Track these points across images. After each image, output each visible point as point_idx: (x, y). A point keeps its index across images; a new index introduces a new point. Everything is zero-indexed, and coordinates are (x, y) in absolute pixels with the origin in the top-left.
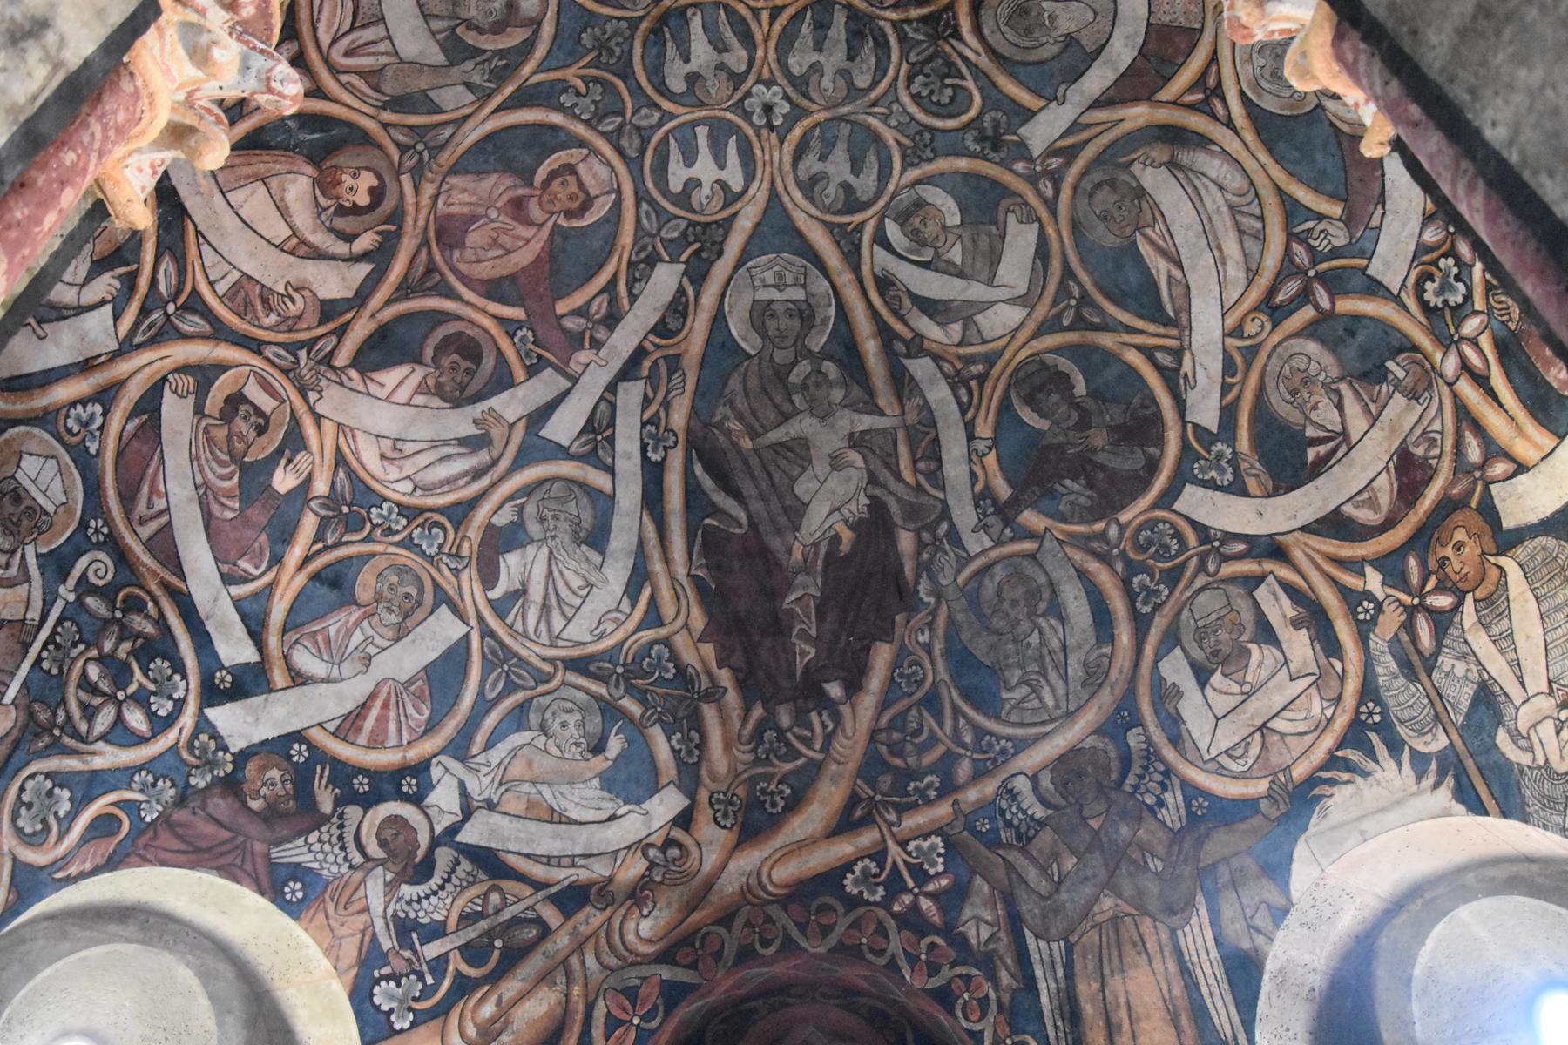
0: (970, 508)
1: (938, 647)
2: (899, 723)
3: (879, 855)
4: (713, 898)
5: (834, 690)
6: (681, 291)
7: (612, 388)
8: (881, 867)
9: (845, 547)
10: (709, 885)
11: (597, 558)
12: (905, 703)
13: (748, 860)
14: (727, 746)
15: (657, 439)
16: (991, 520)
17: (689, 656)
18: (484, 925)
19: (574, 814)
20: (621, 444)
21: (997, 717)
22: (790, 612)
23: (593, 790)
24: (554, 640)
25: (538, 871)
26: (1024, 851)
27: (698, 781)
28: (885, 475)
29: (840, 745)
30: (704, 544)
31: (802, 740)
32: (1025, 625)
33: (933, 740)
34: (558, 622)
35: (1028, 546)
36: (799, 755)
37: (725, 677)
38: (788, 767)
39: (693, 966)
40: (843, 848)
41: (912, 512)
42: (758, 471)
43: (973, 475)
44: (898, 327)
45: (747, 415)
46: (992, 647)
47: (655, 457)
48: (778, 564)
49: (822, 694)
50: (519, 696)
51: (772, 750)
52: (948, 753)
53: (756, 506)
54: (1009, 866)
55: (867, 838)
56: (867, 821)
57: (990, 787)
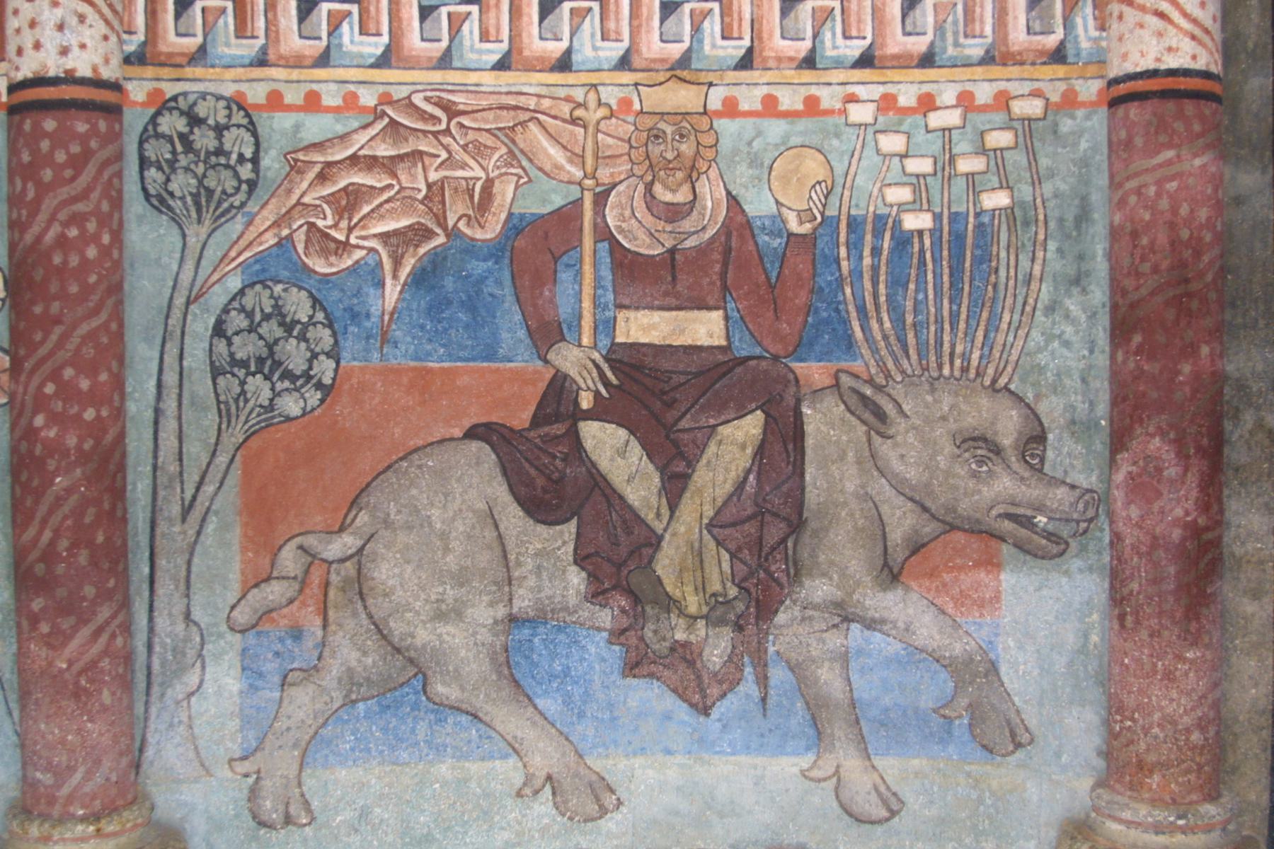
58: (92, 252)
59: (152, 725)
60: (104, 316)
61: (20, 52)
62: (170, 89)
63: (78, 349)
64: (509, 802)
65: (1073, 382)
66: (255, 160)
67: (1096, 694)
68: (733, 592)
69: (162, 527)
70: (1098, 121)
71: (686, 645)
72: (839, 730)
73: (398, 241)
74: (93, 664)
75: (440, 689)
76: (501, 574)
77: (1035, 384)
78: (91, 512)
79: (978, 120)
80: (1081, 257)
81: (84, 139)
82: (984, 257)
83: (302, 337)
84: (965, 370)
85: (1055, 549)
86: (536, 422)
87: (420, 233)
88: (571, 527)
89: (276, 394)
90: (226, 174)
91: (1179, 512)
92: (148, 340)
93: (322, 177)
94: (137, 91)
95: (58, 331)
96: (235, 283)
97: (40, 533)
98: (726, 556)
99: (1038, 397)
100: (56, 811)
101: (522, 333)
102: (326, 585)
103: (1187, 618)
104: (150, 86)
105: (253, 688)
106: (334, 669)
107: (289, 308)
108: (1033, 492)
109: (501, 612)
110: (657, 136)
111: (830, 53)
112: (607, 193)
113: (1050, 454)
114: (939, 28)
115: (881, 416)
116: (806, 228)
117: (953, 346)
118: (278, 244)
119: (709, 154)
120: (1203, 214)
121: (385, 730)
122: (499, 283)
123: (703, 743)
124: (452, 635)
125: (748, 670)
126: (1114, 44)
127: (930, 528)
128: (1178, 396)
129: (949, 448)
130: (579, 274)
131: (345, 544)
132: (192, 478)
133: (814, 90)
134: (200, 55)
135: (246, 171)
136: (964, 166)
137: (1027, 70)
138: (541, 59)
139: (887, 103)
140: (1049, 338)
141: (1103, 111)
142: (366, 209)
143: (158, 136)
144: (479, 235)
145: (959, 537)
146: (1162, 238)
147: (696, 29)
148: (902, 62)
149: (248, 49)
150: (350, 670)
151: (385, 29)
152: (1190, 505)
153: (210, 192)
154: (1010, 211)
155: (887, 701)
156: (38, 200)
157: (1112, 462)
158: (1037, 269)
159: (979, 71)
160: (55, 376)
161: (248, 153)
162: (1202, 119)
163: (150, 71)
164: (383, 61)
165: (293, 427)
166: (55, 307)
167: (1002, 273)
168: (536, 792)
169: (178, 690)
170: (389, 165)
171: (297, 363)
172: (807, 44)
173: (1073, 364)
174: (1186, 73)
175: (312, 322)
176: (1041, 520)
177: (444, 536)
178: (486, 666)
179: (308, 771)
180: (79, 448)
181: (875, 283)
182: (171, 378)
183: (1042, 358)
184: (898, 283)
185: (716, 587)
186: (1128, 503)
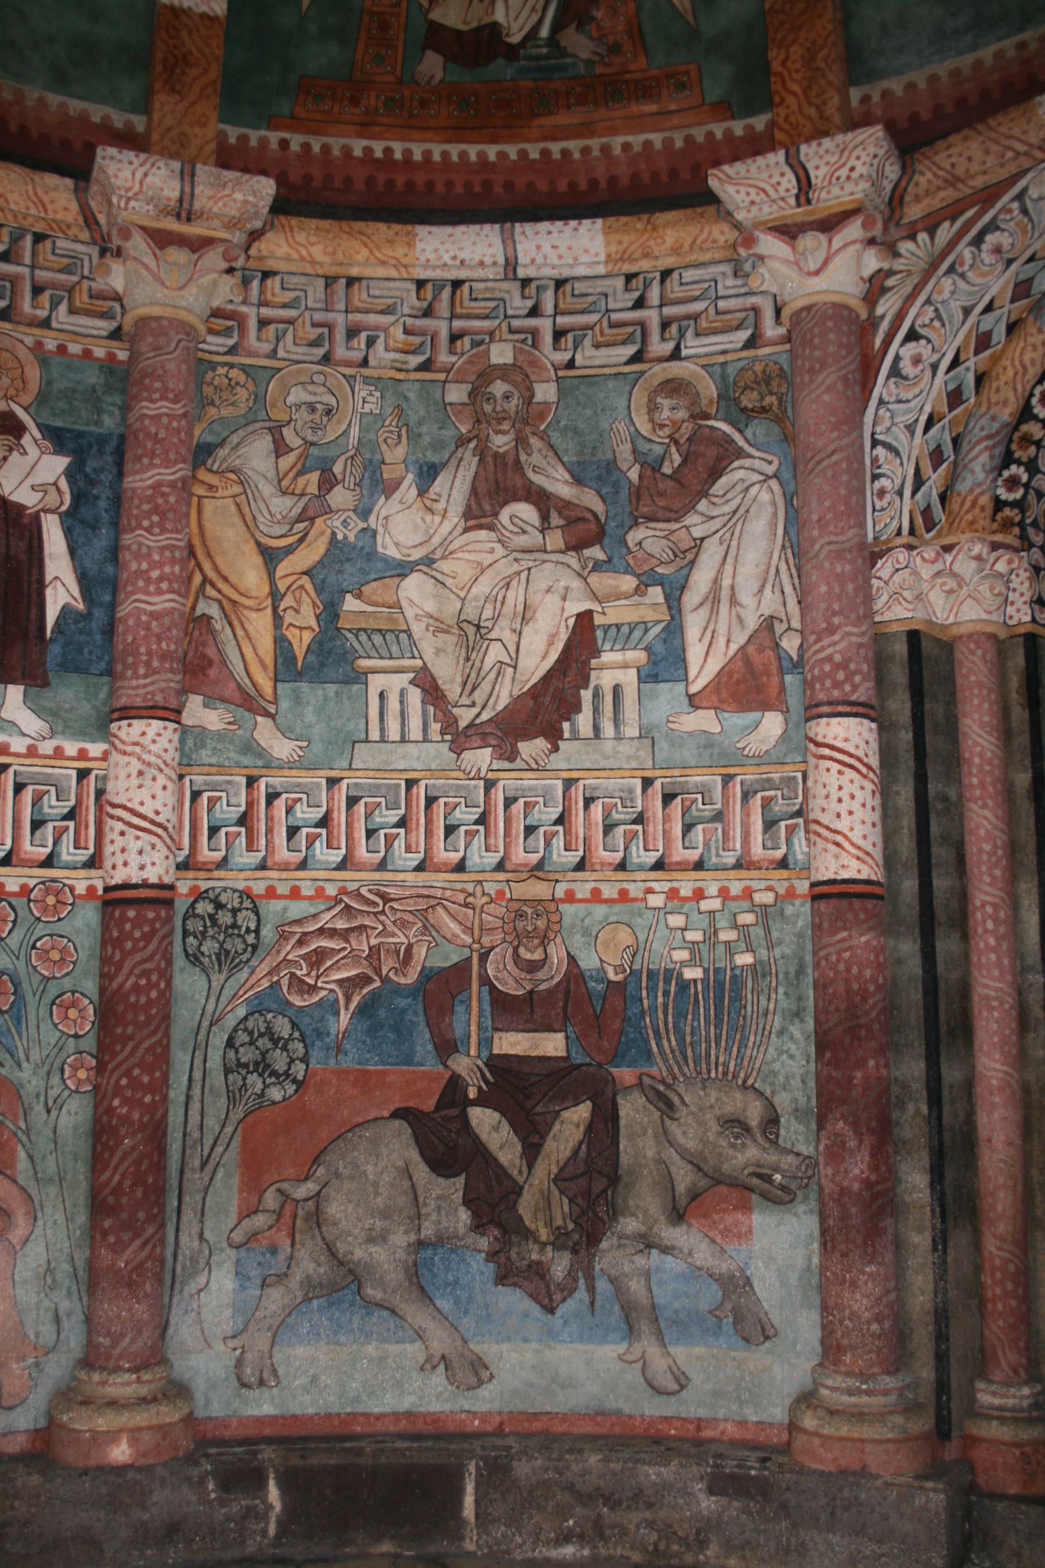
58: (154, 994)
59: (173, 1311)
60: (159, 1035)
61: (114, 867)
62: (204, 885)
63: (143, 1058)
64: (415, 1375)
65: (796, 1083)
66: (257, 931)
68: (571, 1226)
69: (188, 1174)
71: (539, 1263)
72: (644, 1326)
73: (349, 985)
74: (140, 1266)
75: (370, 1291)
76: (413, 1212)
77: (772, 1084)
78: (146, 1162)
79: (733, 906)
80: (800, 998)
81: (152, 923)
82: (737, 998)
83: (285, 1049)
85: (787, 1198)
86: (439, 1107)
87: (363, 980)
88: (461, 1181)
89: (266, 1086)
90: (238, 940)
91: (856, 1171)
92: (184, 1050)
93: (300, 943)
94: (183, 888)
95: (131, 1044)
96: (241, 1012)
97: (112, 1176)
98: (566, 1201)
99: (773, 1093)
100: (111, 1364)
101: (430, 1047)
102: (295, 1216)
104: (190, 883)
105: (243, 1288)
106: (298, 1275)
107: (276, 1029)
108: (773, 1158)
109: (412, 1237)
110: (521, 915)
111: (635, 860)
112: (488, 953)
113: (782, 1132)
114: (707, 844)
115: (670, 1105)
116: (620, 977)
118: (271, 987)
119: (556, 927)
120: (868, 973)
121: (330, 1319)
122: (416, 1013)
123: (550, 1335)
124: (379, 1253)
125: (582, 1282)
127: (704, 1183)
128: (854, 1093)
129: (715, 1127)
130: (469, 1007)
131: (309, 1188)
132: (208, 1142)
133: (625, 885)
134: (223, 863)
135: (251, 939)
136: (723, 936)
137: (763, 873)
138: (445, 864)
139: (673, 894)
140: (780, 1052)
142: (329, 963)
143: (195, 916)
144: (403, 981)
145: (724, 1189)
146: (841, 988)
147: (548, 844)
148: (683, 867)
149: (255, 858)
150: (308, 1277)
151: (343, 844)
152: (864, 1167)
153: (227, 952)
154: (753, 967)
155: (677, 1305)
156: (122, 961)
158: (772, 1006)
159: (732, 874)
160: (128, 1073)
161: (253, 927)
162: (865, 910)
163: (191, 874)
164: (342, 866)
165: (276, 1108)
166: (130, 1029)
168: (434, 1367)
169: (192, 1287)
170: (344, 935)
171: (280, 1066)
172: (621, 854)
173: (796, 1070)
174: (854, 881)
175: (291, 1038)
176: (778, 1177)
177: (375, 1184)
178: (402, 1276)
179: (276, 1348)
180: (140, 1120)
181: (666, 1015)
182: (198, 1075)
183: (777, 1066)
184: (681, 1015)
185: (559, 1222)
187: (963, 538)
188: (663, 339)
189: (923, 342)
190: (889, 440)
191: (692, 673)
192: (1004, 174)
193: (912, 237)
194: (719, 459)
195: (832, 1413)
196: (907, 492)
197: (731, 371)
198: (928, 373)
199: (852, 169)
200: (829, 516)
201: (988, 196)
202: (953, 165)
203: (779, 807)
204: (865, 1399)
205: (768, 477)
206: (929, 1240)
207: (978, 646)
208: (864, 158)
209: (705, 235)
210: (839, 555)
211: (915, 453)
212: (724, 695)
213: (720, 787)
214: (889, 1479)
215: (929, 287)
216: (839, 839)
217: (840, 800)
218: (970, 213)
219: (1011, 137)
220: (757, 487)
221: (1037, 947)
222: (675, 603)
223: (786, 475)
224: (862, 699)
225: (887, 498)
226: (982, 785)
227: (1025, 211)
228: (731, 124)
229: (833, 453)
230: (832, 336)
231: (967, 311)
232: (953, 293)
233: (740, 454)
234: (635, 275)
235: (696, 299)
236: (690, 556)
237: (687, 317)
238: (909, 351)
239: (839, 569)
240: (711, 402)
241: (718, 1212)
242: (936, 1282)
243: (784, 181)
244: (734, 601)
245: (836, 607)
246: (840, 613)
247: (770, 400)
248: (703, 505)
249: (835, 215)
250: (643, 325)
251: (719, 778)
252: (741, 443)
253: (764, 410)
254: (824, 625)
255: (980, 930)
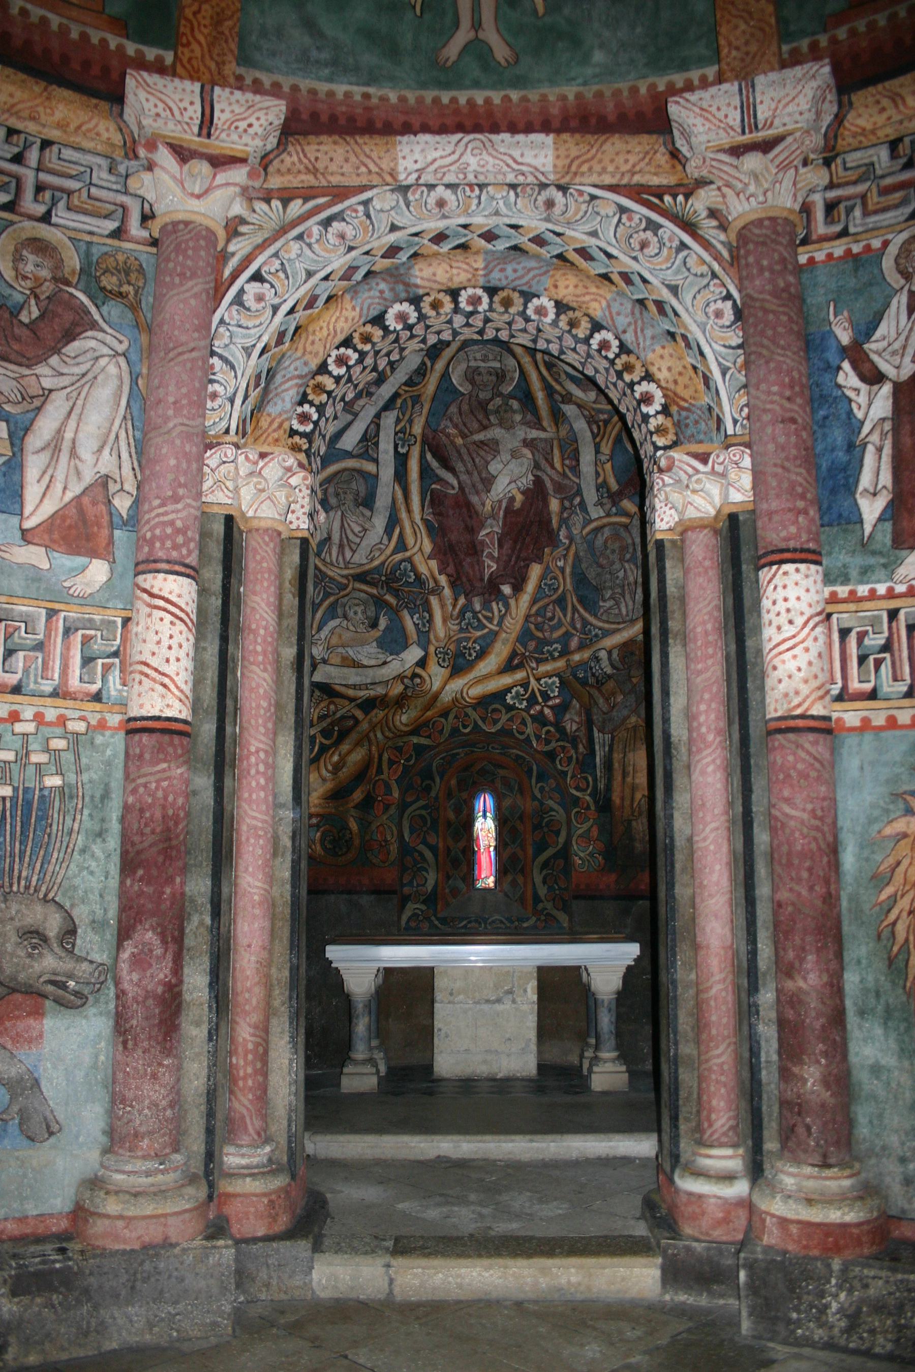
0: (594, 490)
1: (568, 570)
2: (541, 613)
3: (525, 685)
4: (438, 704)
5: (507, 589)
6: (423, 363)
7: (378, 416)
8: (526, 691)
9: (517, 505)
10: (436, 696)
11: (368, 513)
12: (546, 600)
13: (457, 684)
14: (445, 621)
15: (404, 441)
16: (605, 501)
17: (423, 569)
18: (329, 720)
19: (365, 662)
20: (382, 446)
21: (595, 616)
22: (482, 543)
23: (372, 648)
24: (347, 564)
25: (351, 693)
26: (600, 691)
27: (429, 642)
28: (543, 463)
29: (508, 621)
30: (432, 502)
31: (486, 617)
32: (617, 566)
33: (560, 624)
34: (348, 554)
35: (624, 520)
36: (485, 627)
37: (443, 580)
38: (479, 634)
39: (429, 737)
40: (507, 680)
41: (559, 488)
42: (466, 457)
43: (597, 473)
44: (558, 387)
45: (461, 426)
46: (598, 575)
47: (402, 450)
48: (476, 513)
49: (499, 591)
50: (332, 599)
51: (469, 624)
52: (567, 633)
53: (463, 477)
54: (591, 696)
55: (520, 675)
56: (520, 666)
57: (586, 654)
65: (94, 897)
67: (103, 1095)
70: (118, 741)
79: (45, 730)
80: (103, 820)
82: (44, 816)
84: (27, 888)
85: (79, 1002)
91: (161, 976)
99: (72, 906)
103: (165, 1040)
113: (78, 942)
114: (26, 671)
117: (20, 872)
120: (180, 801)
126: (135, 697)
128: (163, 907)
129: (14, 938)
136: (35, 758)
140: (81, 869)
141: (122, 734)
145: (18, 997)
146: (158, 814)
152: (167, 971)
154: (62, 788)
157: (119, 946)
159: (49, 701)
162: (182, 745)
167: (55, 827)
174: (176, 720)
176: (72, 984)
183: (77, 881)
186: (130, 972)
187: (277, 450)
188: (36, 200)
189: (267, 285)
190: (226, 354)
191: (28, 510)
192: (356, 182)
193: (268, 201)
194: (75, 324)
195: (136, 1195)
196: (238, 401)
197: (96, 251)
198: (269, 312)
199: (250, 125)
200: (184, 402)
201: (340, 193)
202: (317, 159)
203: (98, 646)
204: (160, 1177)
205: (117, 354)
206: (206, 1032)
207: (271, 540)
208: (263, 121)
209: (91, 125)
210: (188, 437)
211: (249, 372)
212: (56, 536)
213: (43, 619)
214: (185, 1245)
215: (278, 244)
216: (166, 681)
217: (170, 648)
218: (321, 200)
219: (369, 157)
220: (106, 359)
221: (290, 789)
222: (18, 442)
223: (133, 357)
224: (194, 564)
225: (219, 401)
226: (264, 653)
227: (368, 216)
228: (125, 42)
229: (193, 350)
230: (203, 253)
231: (310, 274)
232: (299, 256)
233: (94, 326)
234: (18, 132)
235: (71, 177)
236: (37, 403)
237: (62, 190)
238: (253, 288)
239: (187, 449)
240: (73, 272)
241: (10, 1019)
242: (209, 1067)
243: (191, 109)
244: (73, 453)
245: (182, 480)
246: (185, 486)
247: (126, 288)
248: (54, 360)
249: (224, 156)
250: (19, 180)
251: (44, 612)
252: (97, 317)
253: (121, 295)
254: (170, 493)
255: (253, 772)
